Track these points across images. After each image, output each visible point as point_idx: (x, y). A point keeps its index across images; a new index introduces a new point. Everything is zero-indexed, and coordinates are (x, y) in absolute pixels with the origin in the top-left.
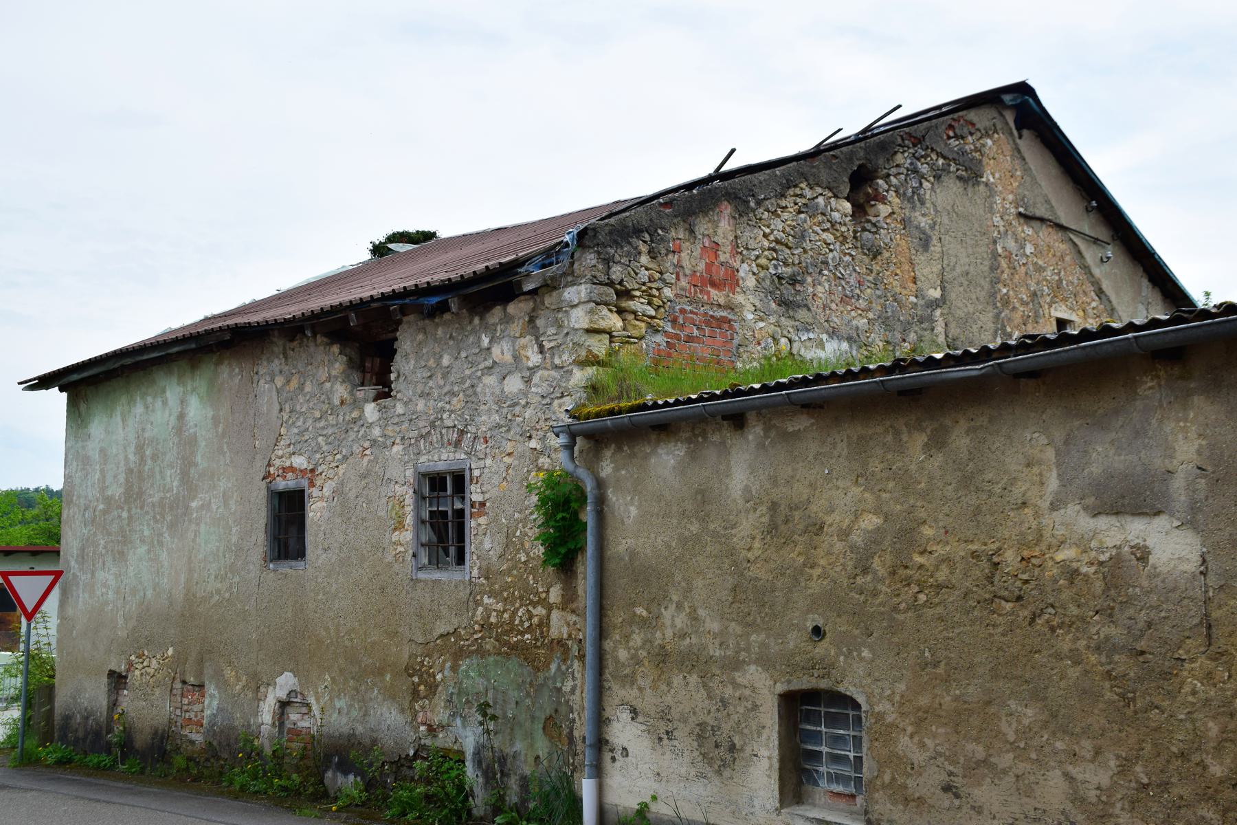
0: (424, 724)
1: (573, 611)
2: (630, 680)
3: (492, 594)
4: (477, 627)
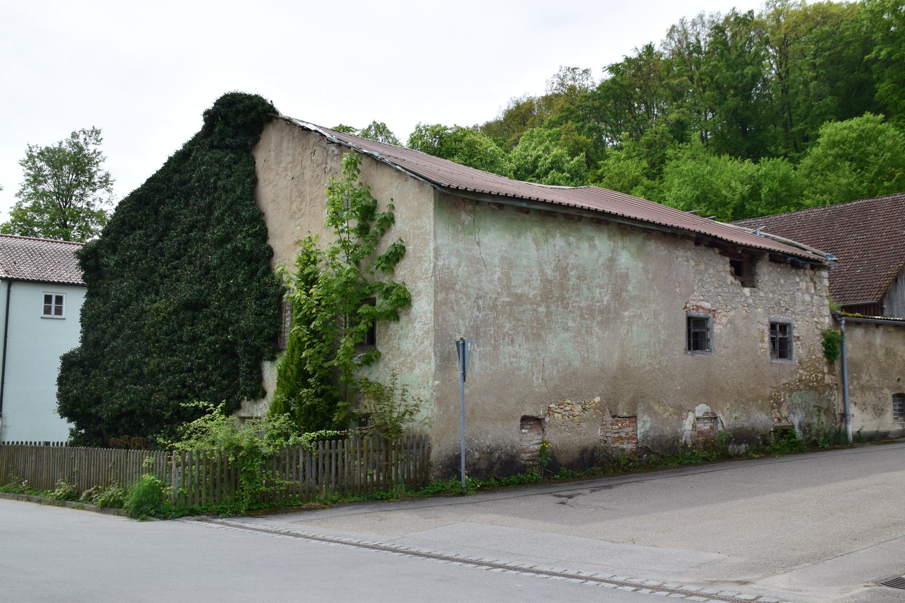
0: (776, 418)
1: (833, 375)
2: (853, 395)
3: (803, 369)
4: (797, 381)
